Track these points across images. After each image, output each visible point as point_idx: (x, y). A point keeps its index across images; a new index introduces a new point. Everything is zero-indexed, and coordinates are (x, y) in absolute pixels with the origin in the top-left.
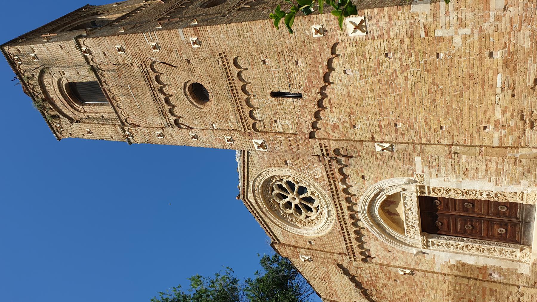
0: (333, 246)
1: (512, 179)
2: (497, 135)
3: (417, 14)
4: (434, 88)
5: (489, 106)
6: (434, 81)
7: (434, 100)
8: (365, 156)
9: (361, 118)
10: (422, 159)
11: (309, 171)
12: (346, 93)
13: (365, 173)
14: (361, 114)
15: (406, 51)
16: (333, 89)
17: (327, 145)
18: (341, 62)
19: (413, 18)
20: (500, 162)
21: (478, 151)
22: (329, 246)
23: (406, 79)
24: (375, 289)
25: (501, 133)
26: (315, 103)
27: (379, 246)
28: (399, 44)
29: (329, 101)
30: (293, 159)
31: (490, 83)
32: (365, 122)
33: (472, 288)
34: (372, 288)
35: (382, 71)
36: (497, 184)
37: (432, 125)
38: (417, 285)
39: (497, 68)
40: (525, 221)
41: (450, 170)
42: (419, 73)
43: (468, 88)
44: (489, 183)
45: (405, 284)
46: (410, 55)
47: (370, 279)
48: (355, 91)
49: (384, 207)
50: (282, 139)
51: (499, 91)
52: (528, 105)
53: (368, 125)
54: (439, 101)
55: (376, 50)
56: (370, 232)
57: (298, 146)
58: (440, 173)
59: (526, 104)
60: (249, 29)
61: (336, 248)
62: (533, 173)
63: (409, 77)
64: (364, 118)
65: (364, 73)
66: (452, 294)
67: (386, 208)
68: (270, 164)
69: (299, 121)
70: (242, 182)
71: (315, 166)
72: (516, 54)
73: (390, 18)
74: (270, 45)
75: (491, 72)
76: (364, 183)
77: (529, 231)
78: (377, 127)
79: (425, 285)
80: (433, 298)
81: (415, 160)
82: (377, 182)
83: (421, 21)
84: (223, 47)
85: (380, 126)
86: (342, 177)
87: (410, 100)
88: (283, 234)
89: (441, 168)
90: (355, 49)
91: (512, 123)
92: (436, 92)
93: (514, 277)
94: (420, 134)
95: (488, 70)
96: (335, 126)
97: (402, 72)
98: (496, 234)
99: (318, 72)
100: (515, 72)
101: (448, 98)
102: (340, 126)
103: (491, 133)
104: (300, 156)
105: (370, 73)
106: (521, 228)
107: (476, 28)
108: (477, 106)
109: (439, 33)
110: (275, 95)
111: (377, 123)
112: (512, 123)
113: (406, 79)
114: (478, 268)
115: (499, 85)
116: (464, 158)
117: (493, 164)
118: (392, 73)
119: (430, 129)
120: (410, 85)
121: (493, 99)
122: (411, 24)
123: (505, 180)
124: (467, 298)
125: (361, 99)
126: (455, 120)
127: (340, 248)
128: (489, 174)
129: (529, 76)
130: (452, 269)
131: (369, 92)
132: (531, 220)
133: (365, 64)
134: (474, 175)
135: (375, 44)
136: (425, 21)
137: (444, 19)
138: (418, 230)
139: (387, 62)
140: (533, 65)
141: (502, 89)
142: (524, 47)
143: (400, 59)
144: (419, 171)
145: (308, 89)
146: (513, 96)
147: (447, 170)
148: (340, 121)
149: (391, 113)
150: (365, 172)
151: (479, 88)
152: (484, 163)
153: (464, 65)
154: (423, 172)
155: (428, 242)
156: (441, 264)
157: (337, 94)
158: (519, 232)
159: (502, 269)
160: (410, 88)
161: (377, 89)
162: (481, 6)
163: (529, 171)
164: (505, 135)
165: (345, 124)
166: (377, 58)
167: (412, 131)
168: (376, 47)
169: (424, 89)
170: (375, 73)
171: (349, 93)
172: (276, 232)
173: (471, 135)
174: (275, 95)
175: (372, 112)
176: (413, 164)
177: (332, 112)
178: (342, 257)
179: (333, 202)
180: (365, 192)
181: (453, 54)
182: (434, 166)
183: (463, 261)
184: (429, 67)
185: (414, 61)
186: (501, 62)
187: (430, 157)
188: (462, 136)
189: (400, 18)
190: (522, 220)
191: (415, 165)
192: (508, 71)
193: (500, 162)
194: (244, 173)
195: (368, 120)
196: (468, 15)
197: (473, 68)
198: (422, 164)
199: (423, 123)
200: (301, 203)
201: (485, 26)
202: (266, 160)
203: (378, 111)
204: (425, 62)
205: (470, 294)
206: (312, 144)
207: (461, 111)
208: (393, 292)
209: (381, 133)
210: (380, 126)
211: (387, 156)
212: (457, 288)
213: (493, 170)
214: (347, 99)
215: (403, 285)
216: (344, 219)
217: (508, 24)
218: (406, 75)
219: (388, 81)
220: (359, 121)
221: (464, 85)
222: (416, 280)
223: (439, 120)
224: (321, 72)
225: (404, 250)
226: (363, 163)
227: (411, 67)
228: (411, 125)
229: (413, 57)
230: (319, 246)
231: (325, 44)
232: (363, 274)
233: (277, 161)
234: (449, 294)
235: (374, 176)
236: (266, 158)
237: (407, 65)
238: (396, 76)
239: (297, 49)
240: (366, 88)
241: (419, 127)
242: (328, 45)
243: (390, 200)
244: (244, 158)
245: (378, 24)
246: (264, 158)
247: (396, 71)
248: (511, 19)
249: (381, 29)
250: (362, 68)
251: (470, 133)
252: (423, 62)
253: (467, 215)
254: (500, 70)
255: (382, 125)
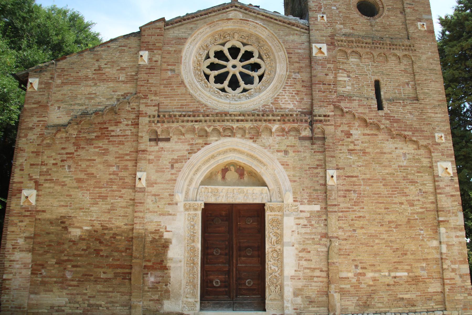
0: (171, 97)
1: (300, 290)
2: (350, 275)
3: (456, 216)
4: (393, 225)
5: (378, 268)
6: (400, 225)
7: (382, 225)
8: (315, 157)
9: (360, 160)
10: (318, 212)
11: (287, 94)
12: (385, 151)
13: (291, 154)
14: (364, 161)
15: (425, 205)
16: (388, 140)
17: (328, 123)
18: (413, 151)
19: (453, 213)
20: (321, 279)
21: (335, 261)
22: (169, 92)
23: (401, 204)
24: (94, 137)
25: (353, 278)
26: (375, 120)
27: (180, 154)
28: (431, 201)
29: (376, 135)
30: (303, 81)
31: (400, 267)
32: (356, 164)
33: (124, 254)
34: (95, 134)
35: (407, 184)
36: (292, 278)
37: (357, 222)
38: (113, 191)
39: (412, 272)
40: (236, 303)
41: (307, 236)
42: (407, 214)
43: (394, 252)
44: (294, 271)
45: (112, 177)
46: (421, 208)
47: (113, 134)
48: (387, 159)
49: (234, 166)
50: (331, 77)
51: (393, 274)
52: (380, 295)
53: (353, 166)
54: (381, 229)
55: (425, 182)
56: (202, 147)
57: (324, 92)
58: (302, 227)
59: (381, 294)
60: (437, 80)
61: (168, 100)
62: (311, 306)
63: (403, 206)
64: (360, 164)
65: (404, 169)
66: (106, 232)
67: (232, 168)
68: (292, 53)
69: (353, 100)
70: (261, 12)
71: (296, 103)
72: (423, 283)
73: (452, 196)
74: (424, 93)
75: (409, 267)
76: (278, 151)
77: (220, 307)
78: (351, 175)
79: (116, 201)
80: (92, 209)
81: (315, 204)
82: (283, 165)
83: (451, 218)
84: (420, 51)
85: (352, 177)
86: (287, 130)
87: (382, 205)
88: (178, 39)
89: (308, 228)
90: (425, 165)
91: (363, 286)
92: (390, 227)
93: (156, 297)
94: (347, 211)
95: (411, 265)
96: (349, 135)
97: (407, 201)
98: (211, 277)
99: (405, 131)
100: (409, 284)
101: (385, 236)
102: (349, 140)
103: (352, 271)
104: (307, 89)
105: (404, 174)
106: (224, 300)
107: (446, 256)
108: (378, 258)
109: (442, 230)
110: (377, 85)
111: (355, 174)
112: (363, 286)
113: (401, 204)
114: (162, 261)
115: (398, 274)
116: (322, 250)
117: (317, 273)
118: (406, 193)
119: (352, 220)
120: (396, 206)
121: (385, 271)
122: (449, 211)
123: (300, 284)
124: (102, 248)
125: (380, 164)
126: (363, 241)
127: (167, 105)
128: (306, 271)
129: (406, 294)
130: (151, 233)
131: (387, 171)
132: (236, 307)
133: (413, 172)
134: (302, 257)
135: (430, 182)
136: (452, 221)
137: (453, 234)
138: (212, 200)
139: (415, 189)
140: (415, 295)
141: (395, 277)
142: (428, 288)
143: (419, 200)
144: (302, 208)
145: (387, 117)
146: (388, 285)
147: (306, 233)
148: (355, 140)
149: (368, 188)
150: (293, 154)
151: (395, 260)
152: (318, 267)
153: (414, 248)
154: (301, 211)
155: (196, 210)
156: (160, 222)
157: (383, 143)
158: (217, 298)
159: (166, 285)
160: (393, 206)
161: (390, 178)
162: (462, 259)
163: (311, 302)
164: (351, 281)
165: (352, 145)
166: (418, 181)
167: (349, 205)
168: (427, 182)
169: (392, 217)
170: (405, 178)
171: (385, 153)
172: (183, 30)
173: (349, 255)
174: (377, 85)
175: (367, 171)
176: (310, 202)
177: (364, 135)
178: (154, 106)
179: (248, 113)
180: (266, 150)
181: (423, 240)
182: (311, 222)
183: (171, 246)
184: (412, 221)
185: (417, 211)
186: (417, 274)
187: (321, 219)
188: (347, 247)
189: (453, 203)
190: (236, 300)
191: (309, 204)
192: (410, 280)
193: (321, 279)
194: (276, 20)
195: (358, 166)
196: (456, 250)
197: (412, 254)
198: (311, 211)
199: (361, 214)
200: (227, 73)
201: (448, 262)
202: (297, 51)
203: (368, 176)
204: (417, 219)
205: (112, 251)
206: (327, 107)
207: (372, 246)
208: (95, 160)
209: (345, 176)
210: (352, 177)
211: (317, 179)
212: (118, 237)
213: (310, 274)
214: (379, 150)
215: (110, 174)
216: (223, 121)
217: (449, 277)
218: (405, 204)
219: (398, 188)
220: (357, 158)
221: (397, 249)
222: (123, 191)
223: (362, 228)
224: (406, 133)
225: (177, 182)
226: (305, 154)
227: (412, 208)
228: (356, 204)
229: (420, 210)
230: (167, 79)
231: (430, 142)
232: (122, 126)
233: (297, 62)
234: (105, 228)
235: (290, 162)
236: (300, 51)
237: (413, 205)
238: (403, 196)
239: (424, 117)
240: (390, 169)
241: (355, 211)
242: (429, 144)
243: (245, 173)
244: (297, 27)
245: (447, 186)
246: (300, 49)
247: (407, 195)
248: (454, 279)
249: (443, 188)
250: (409, 169)
251: (350, 254)
252: (416, 217)
253: (235, 251)
254: (411, 274)
255: (354, 179)
